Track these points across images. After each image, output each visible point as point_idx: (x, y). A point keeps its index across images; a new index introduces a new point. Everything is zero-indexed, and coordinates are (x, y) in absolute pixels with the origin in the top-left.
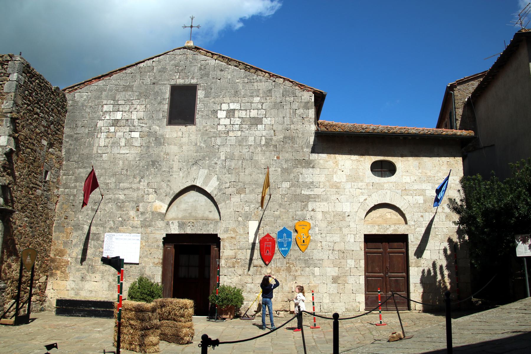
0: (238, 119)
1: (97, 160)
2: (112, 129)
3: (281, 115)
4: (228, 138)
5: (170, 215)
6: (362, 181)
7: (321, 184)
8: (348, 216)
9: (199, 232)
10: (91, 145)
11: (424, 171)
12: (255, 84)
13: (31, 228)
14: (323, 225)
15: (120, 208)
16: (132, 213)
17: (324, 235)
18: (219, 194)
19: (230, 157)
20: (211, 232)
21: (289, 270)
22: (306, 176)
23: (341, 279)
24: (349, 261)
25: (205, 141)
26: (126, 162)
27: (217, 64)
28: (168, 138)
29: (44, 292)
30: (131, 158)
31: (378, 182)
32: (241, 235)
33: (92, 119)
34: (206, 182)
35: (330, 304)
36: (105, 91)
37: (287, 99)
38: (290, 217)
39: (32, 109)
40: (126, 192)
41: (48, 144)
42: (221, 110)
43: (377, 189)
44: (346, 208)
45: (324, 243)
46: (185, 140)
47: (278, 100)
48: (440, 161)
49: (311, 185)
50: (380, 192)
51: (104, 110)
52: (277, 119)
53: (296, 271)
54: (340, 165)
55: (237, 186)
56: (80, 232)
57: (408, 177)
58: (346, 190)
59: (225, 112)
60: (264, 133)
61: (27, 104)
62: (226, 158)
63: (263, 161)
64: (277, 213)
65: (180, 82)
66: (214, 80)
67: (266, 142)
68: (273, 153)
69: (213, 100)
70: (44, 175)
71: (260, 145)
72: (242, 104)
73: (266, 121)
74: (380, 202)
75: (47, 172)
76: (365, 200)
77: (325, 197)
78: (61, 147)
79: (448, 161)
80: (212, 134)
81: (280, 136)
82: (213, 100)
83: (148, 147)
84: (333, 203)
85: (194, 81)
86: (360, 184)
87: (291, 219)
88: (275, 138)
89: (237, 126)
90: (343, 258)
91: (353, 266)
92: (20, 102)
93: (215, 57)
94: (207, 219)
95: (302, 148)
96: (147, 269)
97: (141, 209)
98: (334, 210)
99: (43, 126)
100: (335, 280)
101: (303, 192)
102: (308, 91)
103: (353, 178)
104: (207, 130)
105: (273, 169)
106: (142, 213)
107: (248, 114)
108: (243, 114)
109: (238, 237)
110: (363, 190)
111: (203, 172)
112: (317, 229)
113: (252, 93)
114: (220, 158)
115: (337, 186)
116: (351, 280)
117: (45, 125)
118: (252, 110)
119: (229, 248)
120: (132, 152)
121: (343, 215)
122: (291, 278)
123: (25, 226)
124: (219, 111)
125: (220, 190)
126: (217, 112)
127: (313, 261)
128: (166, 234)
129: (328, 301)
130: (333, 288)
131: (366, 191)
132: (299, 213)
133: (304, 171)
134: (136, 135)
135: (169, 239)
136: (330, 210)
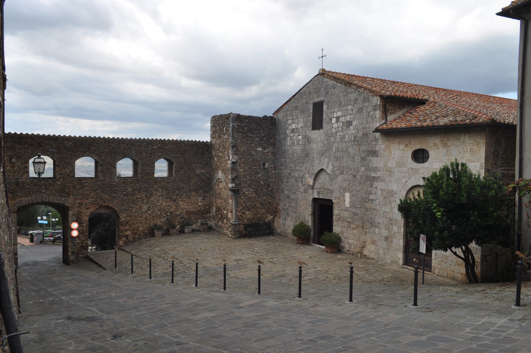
0: (341, 123)
1: (287, 154)
2: (292, 134)
3: (361, 118)
4: (337, 137)
5: (316, 186)
6: (405, 167)
7: (381, 168)
8: (396, 193)
9: (325, 198)
10: (285, 145)
11: (450, 158)
12: (349, 95)
13: (256, 193)
14: (381, 199)
15: (296, 181)
16: (300, 184)
17: (381, 206)
18: (333, 174)
19: (338, 150)
20: (329, 198)
21: (363, 227)
22: (373, 162)
23: (389, 239)
24: (394, 227)
25: (327, 140)
26: (298, 154)
27: (332, 83)
28: (312, 139)
29: (273, 224)
30: (299, 151)
31: (415, 167)
32: (342, 201)
33: (285, 129)
34: (327, 167)
35: (383, 255)
36: (288, 111)
37: (365, 104)
38: (365, 191)
39: (246, 136)
40: (298, 172)
41: (262, 149)
42: (333, 117)
43: (414, 173)
44: (394, 187)
45: (381, 212)
46: (319, 139)
47: (360, 107)
48: (465, 148)
49: (376, 169)
50: (416, 175)
51: (289, 123)
52: (359, 120)
53: (367, 229)
54: (392, 154)
55: (340, 169)
56: (283, 194)
57: (437, 163)
58: (396, 174)
59: (335, 119)
60: (353, 132)
61: (242, 135)
62: (336, 151)
63: (352, 152)
64: (358, 188)
65: (317, 100)
66: (331, 96)
67: (354, 139)
68: (357, 146)
69: (330, 111)
70: (262, 166)
71: (351, 141)
72: (343, 112)
73: (354, 123)
74: (415, 184)
75: (264, 164)
76: (406, 182)
77: (383, 178)
78: (275, 147)
79: (472, 147)
80: (330, 135)
81: (361, 134)
82: (330, 111)
83: (305, 145)
84: (387, 183)
85: (322, 99)
86: (404, 169)
87: (365, 193)
88: (358, 135)
89: (340, 128)
90: (391, 224)
91: (396, 231)
92: (237, 136)
93: (331, 78)
94: (329, 190)
95: (372, 142)
96: (306, 217)
97: (303, 183)
98: (387, 189)
99: (256, 141)
100: (386, 239)
101: (371, 175)
102: (377, 96)
103: (400, 164)
104: (327, 132)
105: (357, 158)
106: (304, 185)
107: (346, 119)
108: (342, 119)
109: (341, 202)
110: (405, 174)
111: (326, 160)
112: (378, 201)
113: (348, 103)
114: (333, 151)
115: (390, 170)
116: (395, 241)
117: (258, 140)
118: (347, 116)
119: (337, 209)
120: (299, 148)
121: (393, 193)
122: (364, 233)
123: (252, 194)
124: (333, 118)
125: (333, 172)
126: (331, 119)
127: (375, 223)
128: (313, 198)
129: (382, 253)
130: (384, 244)
131: (407, 175)
132: (369, 189)
133: (372, 159)
134: (300, 137)
135: (315, 200)
136: (385, 188)
